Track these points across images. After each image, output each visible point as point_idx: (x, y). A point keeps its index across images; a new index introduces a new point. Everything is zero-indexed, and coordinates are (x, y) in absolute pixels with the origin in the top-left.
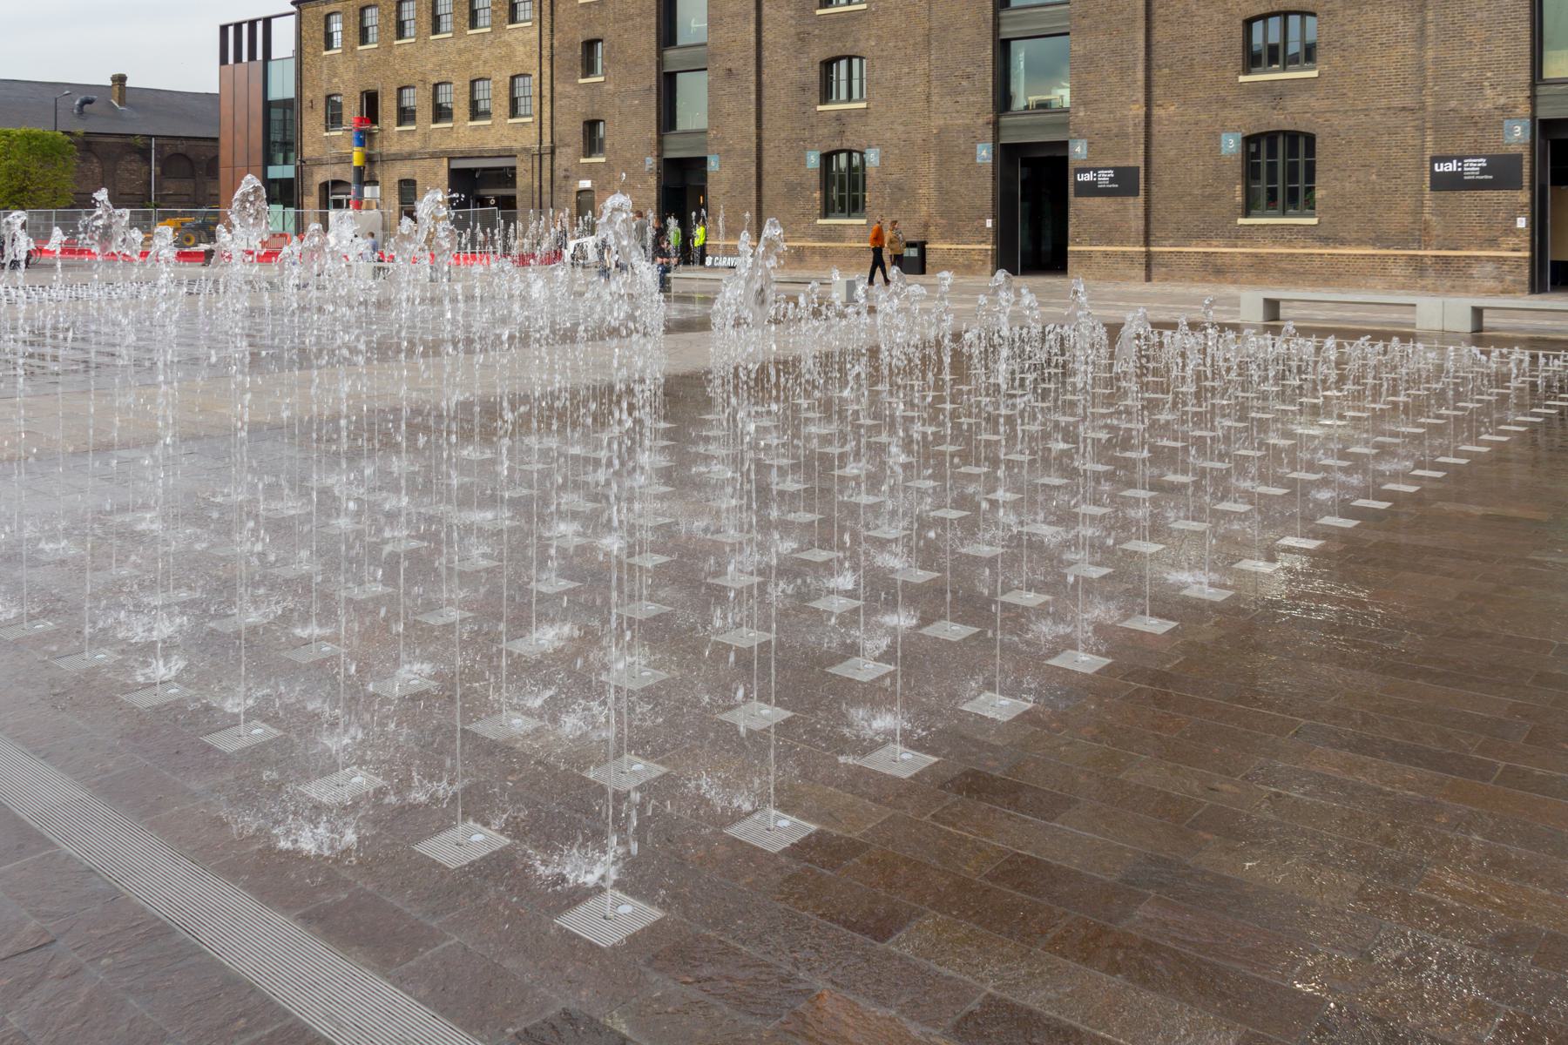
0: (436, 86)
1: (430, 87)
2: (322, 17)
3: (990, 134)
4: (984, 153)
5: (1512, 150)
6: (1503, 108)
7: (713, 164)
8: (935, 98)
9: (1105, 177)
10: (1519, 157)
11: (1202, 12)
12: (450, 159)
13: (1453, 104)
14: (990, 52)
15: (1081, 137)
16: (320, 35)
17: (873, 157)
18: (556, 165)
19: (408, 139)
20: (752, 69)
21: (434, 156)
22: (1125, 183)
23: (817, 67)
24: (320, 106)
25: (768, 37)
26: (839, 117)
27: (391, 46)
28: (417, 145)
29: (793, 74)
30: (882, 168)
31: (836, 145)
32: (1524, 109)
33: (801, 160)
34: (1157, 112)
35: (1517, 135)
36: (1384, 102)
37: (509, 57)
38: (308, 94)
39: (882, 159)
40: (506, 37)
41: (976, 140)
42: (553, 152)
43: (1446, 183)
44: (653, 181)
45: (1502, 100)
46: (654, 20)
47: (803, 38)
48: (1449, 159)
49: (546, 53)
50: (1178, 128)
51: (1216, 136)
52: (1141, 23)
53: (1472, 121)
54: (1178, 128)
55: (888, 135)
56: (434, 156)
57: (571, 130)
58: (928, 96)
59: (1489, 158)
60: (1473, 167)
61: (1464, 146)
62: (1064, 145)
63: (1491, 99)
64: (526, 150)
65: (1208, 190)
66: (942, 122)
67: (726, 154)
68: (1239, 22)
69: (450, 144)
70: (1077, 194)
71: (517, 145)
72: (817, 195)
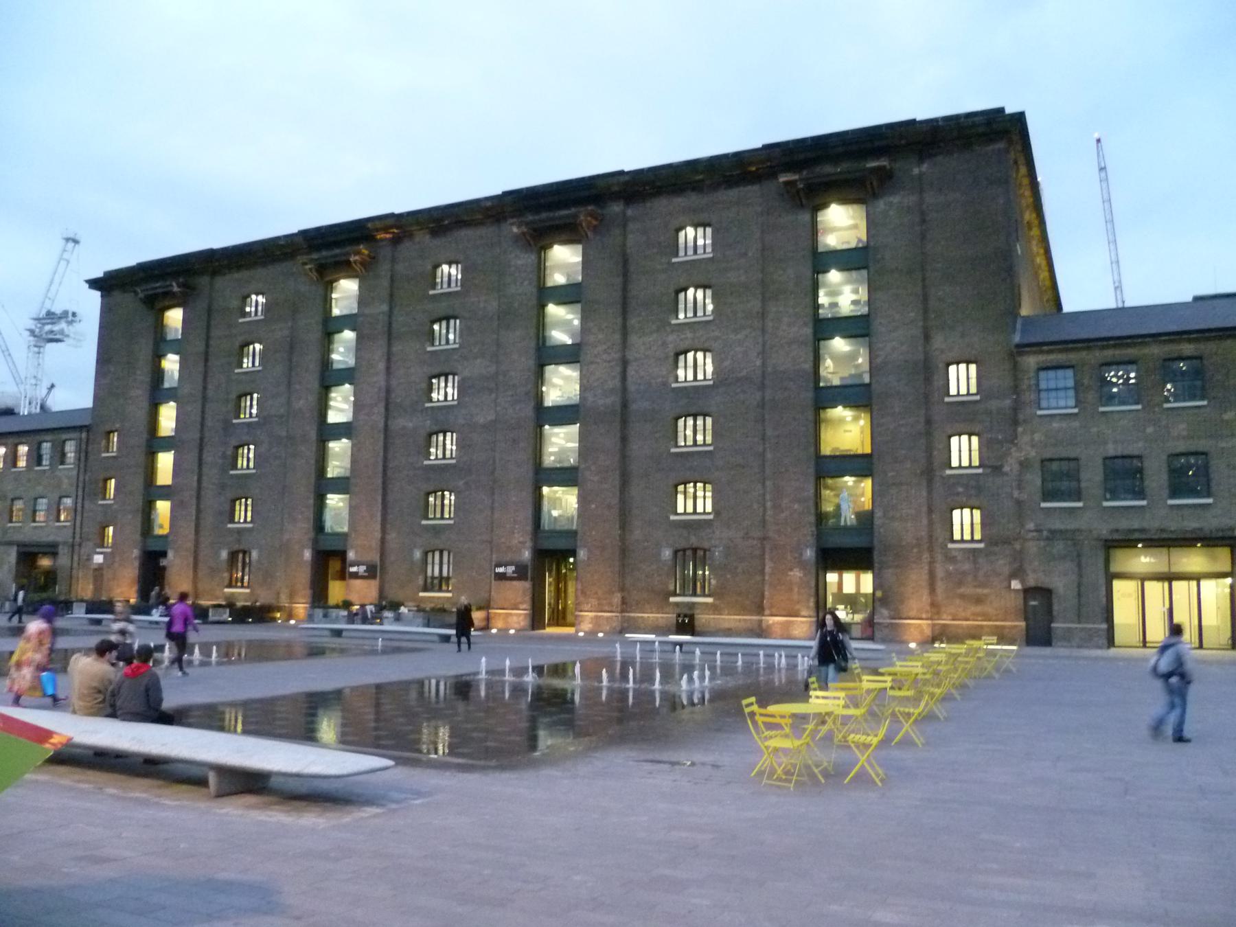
3: (310, 544)
4: (307, 554)
7: (170, 554)
9: (362, 569)
10: (525, 567)
21: (10, 543)
22: (371, 573)
30: (259, 561)
31: (236, 547)
32: (529, 544)
33: (217, 554)
34: (388, 537)
35: (527, 555)
37: (59, 486)
40: (57, 473)
41: (303, 547)
42: (80, 545)
43: (502, 577)
47: (223, 487)
48: (500, 565)
49: (81, 485)
52: (380, 492)
53: (509, 548)
56: (10, 543)
59: (517, 567)
60: (511, 569)
61: (508, 558)
64: (65, 543)
68: (422, 493)
69: (19, 537)
71: (59, 539)
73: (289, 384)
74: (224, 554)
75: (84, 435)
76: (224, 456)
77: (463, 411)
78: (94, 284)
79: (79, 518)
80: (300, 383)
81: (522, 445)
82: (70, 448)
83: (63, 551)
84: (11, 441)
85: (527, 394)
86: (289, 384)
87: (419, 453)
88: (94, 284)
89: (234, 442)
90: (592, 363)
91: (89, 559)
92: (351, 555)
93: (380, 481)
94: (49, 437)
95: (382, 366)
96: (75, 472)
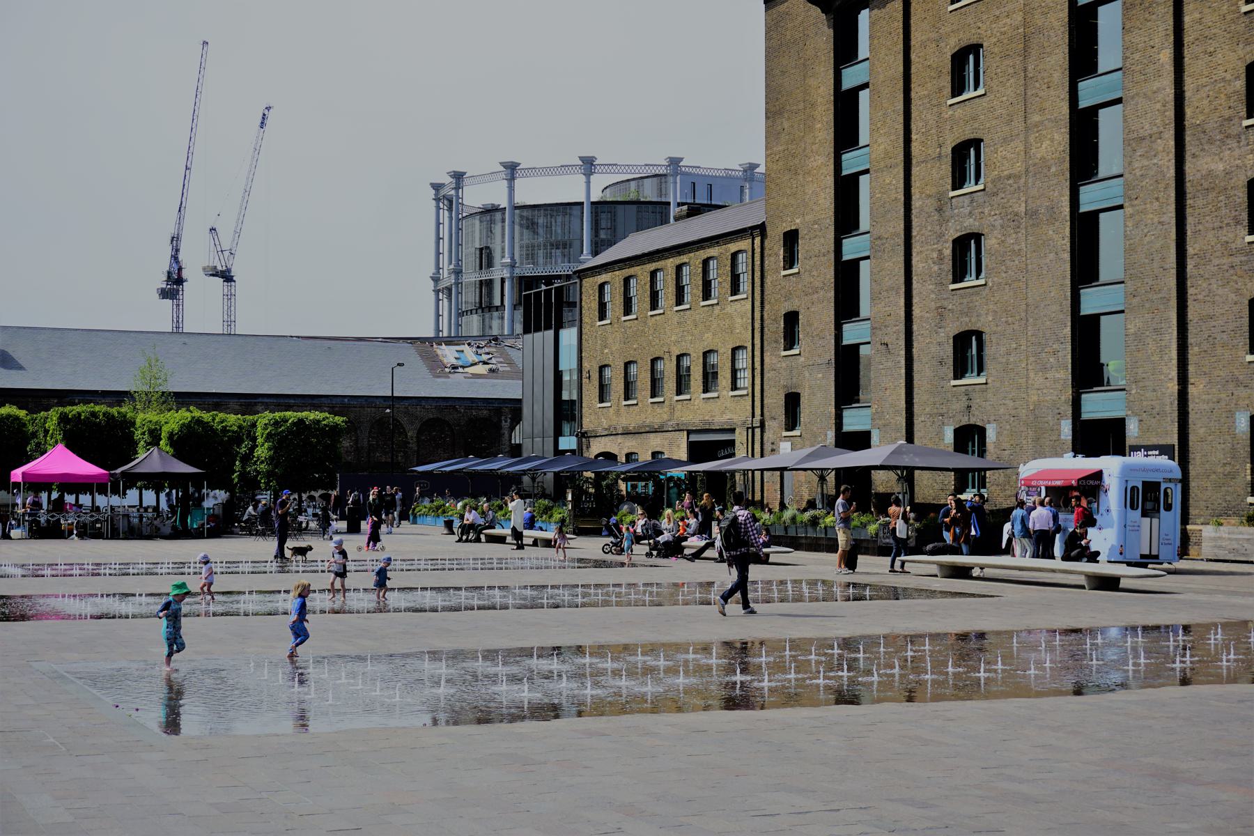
0: (679, 357)
1: (674, 359)
2: (596, 287)
8: (1032, 375)
11: (1220, 292)
12: (689, 432)
14: (1069, 329)
16: (595, 305)
18: (765, 439)
19: (659, 410)
20: (902, 343)
23: (951, 341)
24: (595, 376)
25: (916, 311)
26: (968, 392)
29: (934, 349)
34: (1192, 390)
38: (586, 364)
39: (999, 434)
46: (832, 293)
47: (941, 312)
49: (757, 325)
50: (1205, 406)
51: (1231, 414)
52: (1174, 303)
54: (1205, 406)
55: (1002, 411)
57: (776, 403)
65: (1228, 469)
66: (1035, 398)
75: (758, 241)
80: (1042, 110)
83: (740, 437)
89: (953, 233)
93: (1172, 282)
95: (1166, 56)
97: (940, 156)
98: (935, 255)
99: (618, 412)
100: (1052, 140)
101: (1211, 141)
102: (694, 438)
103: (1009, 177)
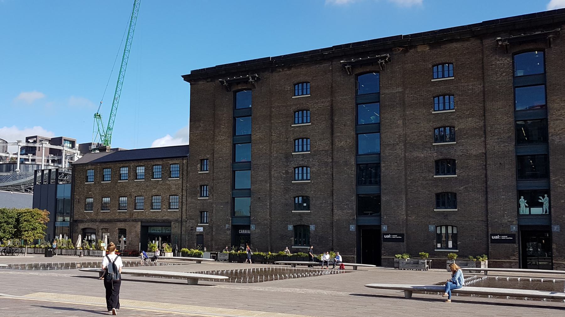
4: (353, 228)
5: (513, 233)
6: (510, 222)
13: (496, 220)
15: (385, 224)
17: (312, 228)
21: (136, 221)
27: (117, 182)
28: (127, 217)
31: (299, 223)
36: (476, 219)
37: (169, 189)
44: (229, 232)
45: (510, 220)
58: (333, 209)
62: (380, 226)
63: (506, 220)
64: (176, 221)
67: (258, 225)
70: (384, 241)
72: (293, 239)
73: (332, 133)
74: (290, 227)
76: (287, 172)
77: (461, 147)
78: (183, 76)
79: (184, 207)
81: (507, 166)
82: (175, 168)
84: (132, 164)
85: (508, 137)
86: (332, 133)
87: (429, 171)
88: (183, 76)
90: (557, 120)
91: (193, 229)
92: (384, 228)
94: (160, 162)
96: (180, 182)
97: (287, 141)
98: (284, 172)
99: (97, 214)
100: (346, 141)
101: (419, 148)
102: (143, 224)
103: (323, 151)
